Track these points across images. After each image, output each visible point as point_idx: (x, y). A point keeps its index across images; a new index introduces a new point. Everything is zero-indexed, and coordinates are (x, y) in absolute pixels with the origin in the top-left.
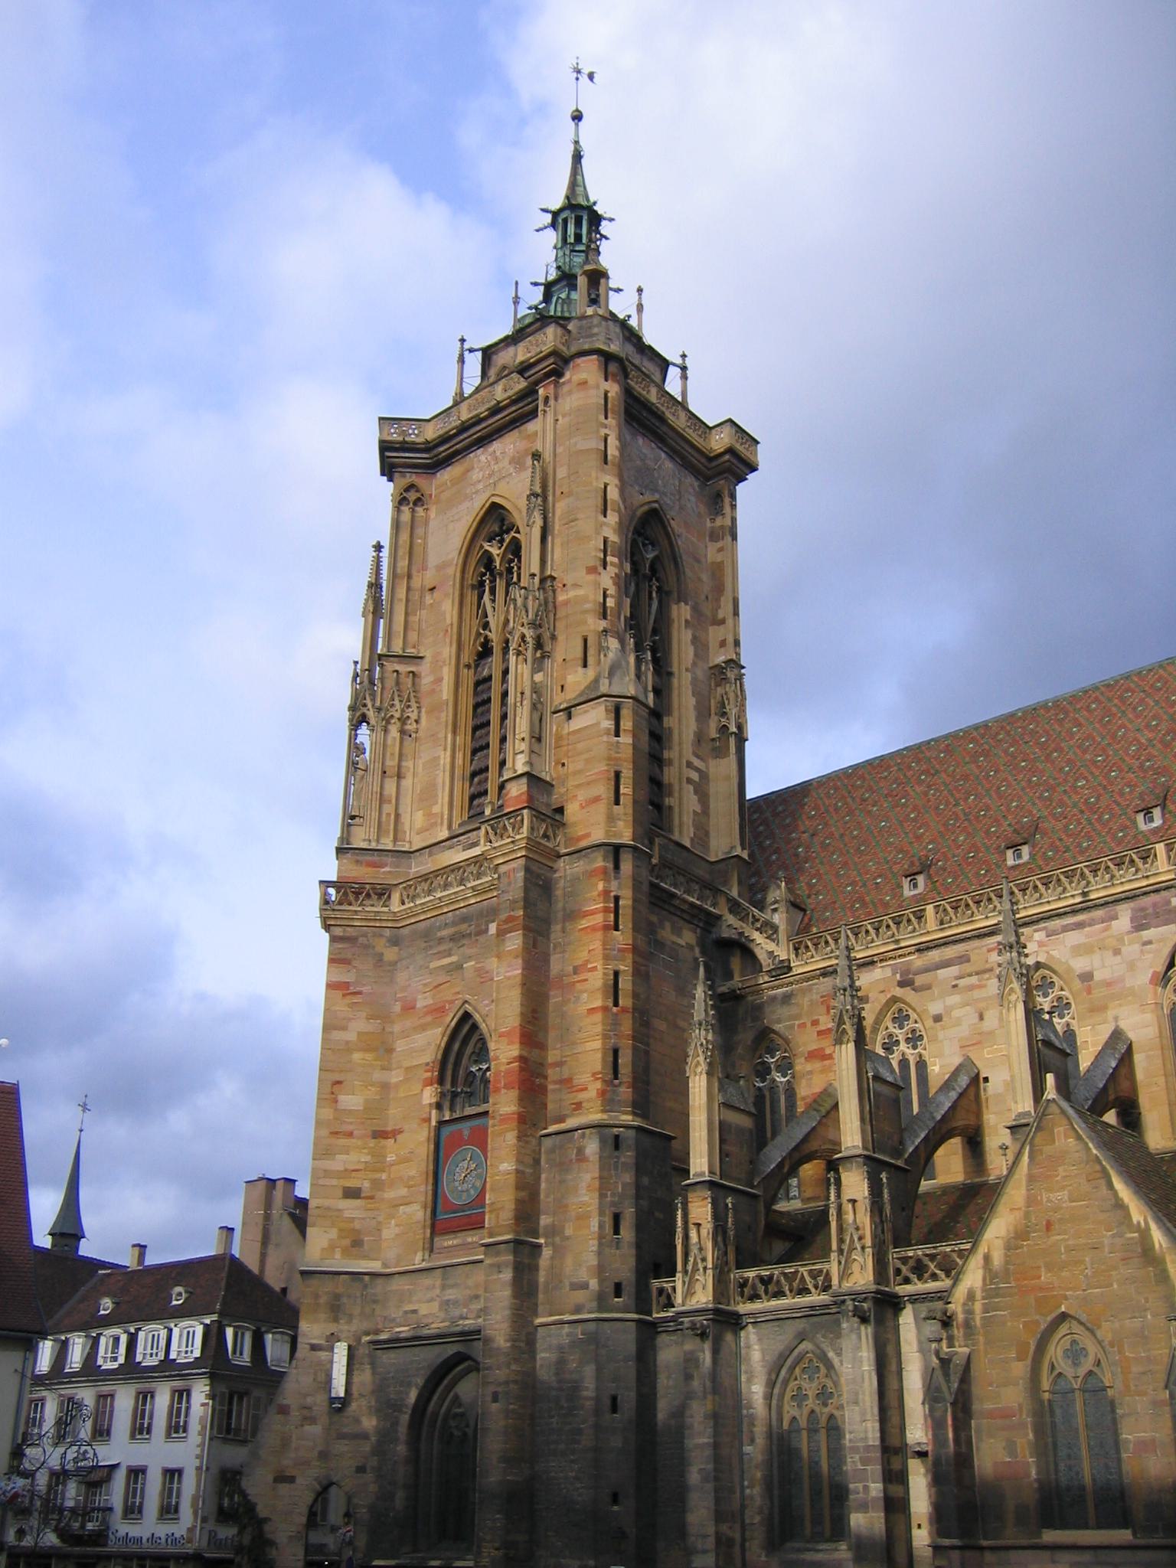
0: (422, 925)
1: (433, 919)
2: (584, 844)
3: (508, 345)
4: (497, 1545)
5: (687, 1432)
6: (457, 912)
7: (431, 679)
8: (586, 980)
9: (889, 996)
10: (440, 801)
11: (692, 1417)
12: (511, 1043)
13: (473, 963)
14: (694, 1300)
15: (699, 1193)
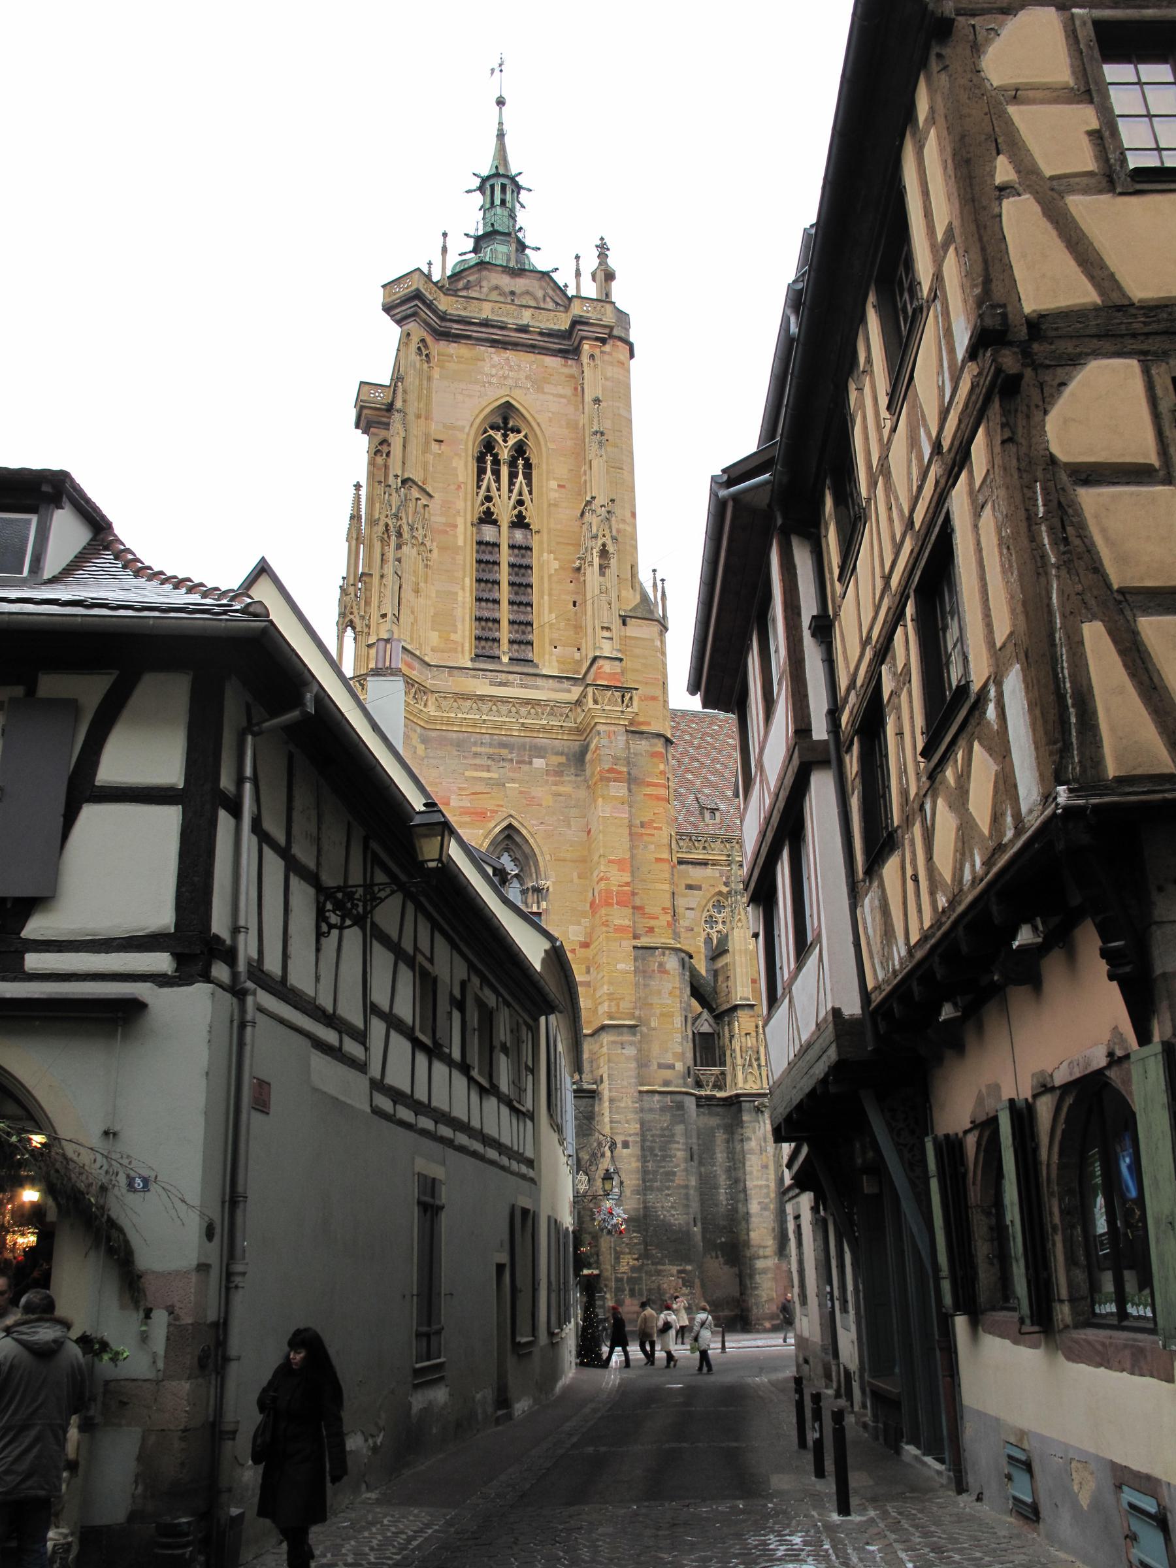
0: (454, 735)
1: (466, 734)
2: (644, 728)
3: (503, 272)
4: (636, 1256)
5: (748, 1177)
6: (495, 737)
7: (443, 520)
8: (653, 835)
9: (717, 890)
10: (459, 632)
11: (751, 1166)
12: (621, 870)
13: (517, 785)
14: (747, 1087)
15: (746, 1012)
